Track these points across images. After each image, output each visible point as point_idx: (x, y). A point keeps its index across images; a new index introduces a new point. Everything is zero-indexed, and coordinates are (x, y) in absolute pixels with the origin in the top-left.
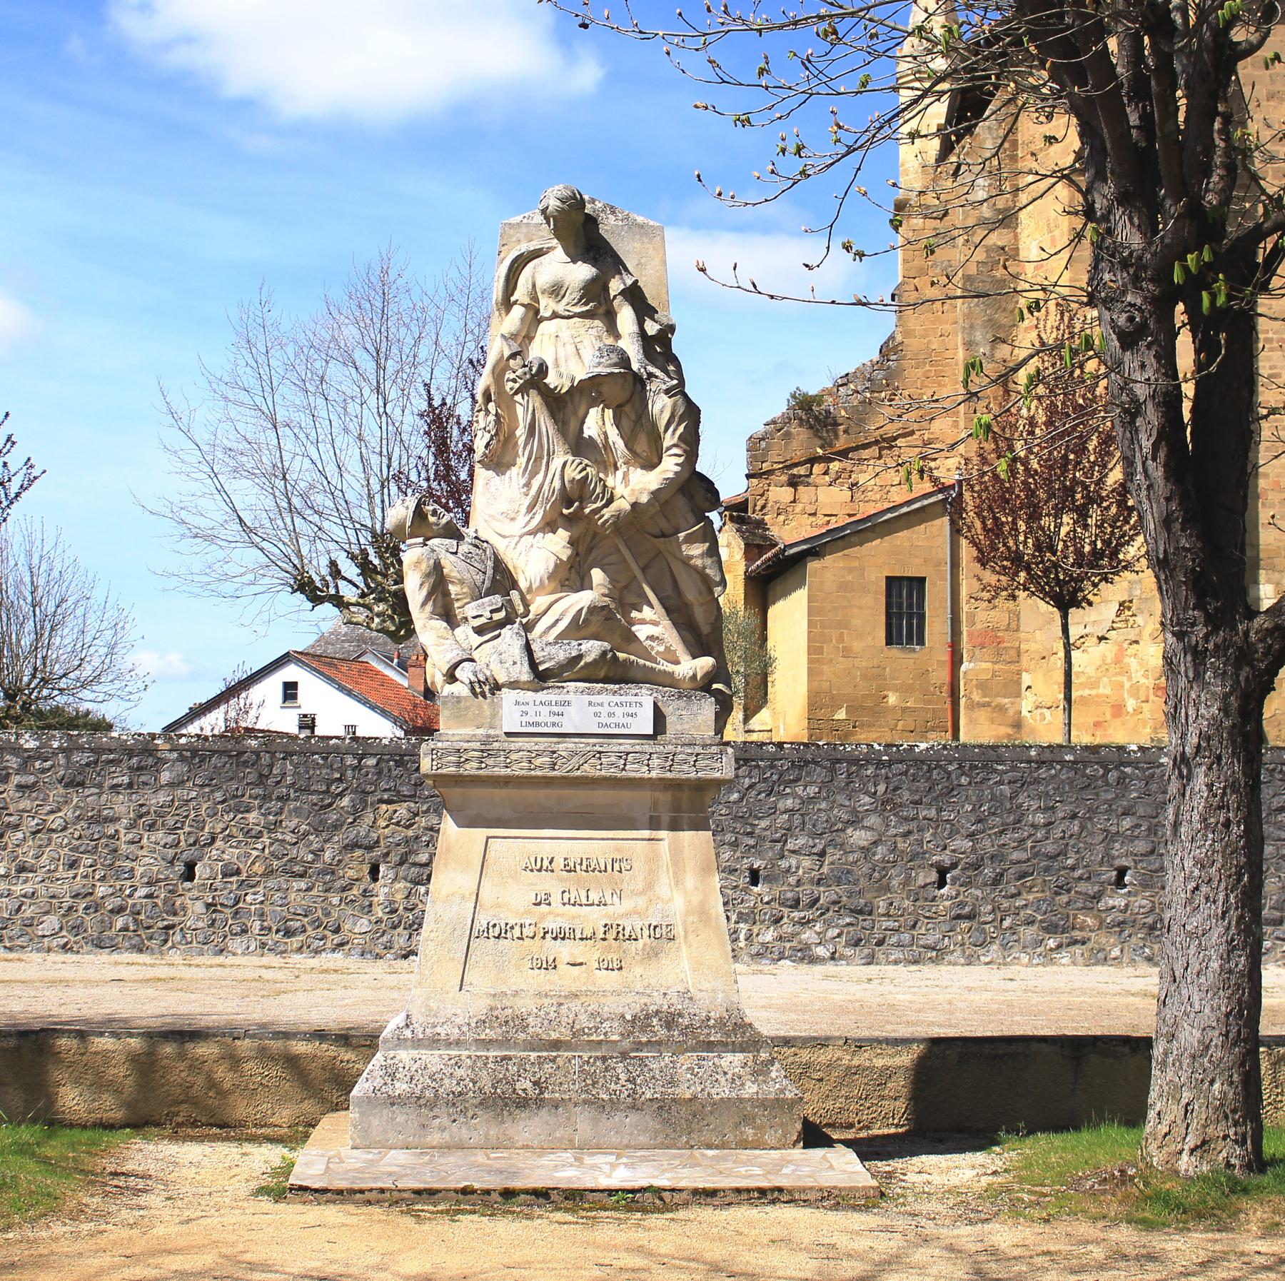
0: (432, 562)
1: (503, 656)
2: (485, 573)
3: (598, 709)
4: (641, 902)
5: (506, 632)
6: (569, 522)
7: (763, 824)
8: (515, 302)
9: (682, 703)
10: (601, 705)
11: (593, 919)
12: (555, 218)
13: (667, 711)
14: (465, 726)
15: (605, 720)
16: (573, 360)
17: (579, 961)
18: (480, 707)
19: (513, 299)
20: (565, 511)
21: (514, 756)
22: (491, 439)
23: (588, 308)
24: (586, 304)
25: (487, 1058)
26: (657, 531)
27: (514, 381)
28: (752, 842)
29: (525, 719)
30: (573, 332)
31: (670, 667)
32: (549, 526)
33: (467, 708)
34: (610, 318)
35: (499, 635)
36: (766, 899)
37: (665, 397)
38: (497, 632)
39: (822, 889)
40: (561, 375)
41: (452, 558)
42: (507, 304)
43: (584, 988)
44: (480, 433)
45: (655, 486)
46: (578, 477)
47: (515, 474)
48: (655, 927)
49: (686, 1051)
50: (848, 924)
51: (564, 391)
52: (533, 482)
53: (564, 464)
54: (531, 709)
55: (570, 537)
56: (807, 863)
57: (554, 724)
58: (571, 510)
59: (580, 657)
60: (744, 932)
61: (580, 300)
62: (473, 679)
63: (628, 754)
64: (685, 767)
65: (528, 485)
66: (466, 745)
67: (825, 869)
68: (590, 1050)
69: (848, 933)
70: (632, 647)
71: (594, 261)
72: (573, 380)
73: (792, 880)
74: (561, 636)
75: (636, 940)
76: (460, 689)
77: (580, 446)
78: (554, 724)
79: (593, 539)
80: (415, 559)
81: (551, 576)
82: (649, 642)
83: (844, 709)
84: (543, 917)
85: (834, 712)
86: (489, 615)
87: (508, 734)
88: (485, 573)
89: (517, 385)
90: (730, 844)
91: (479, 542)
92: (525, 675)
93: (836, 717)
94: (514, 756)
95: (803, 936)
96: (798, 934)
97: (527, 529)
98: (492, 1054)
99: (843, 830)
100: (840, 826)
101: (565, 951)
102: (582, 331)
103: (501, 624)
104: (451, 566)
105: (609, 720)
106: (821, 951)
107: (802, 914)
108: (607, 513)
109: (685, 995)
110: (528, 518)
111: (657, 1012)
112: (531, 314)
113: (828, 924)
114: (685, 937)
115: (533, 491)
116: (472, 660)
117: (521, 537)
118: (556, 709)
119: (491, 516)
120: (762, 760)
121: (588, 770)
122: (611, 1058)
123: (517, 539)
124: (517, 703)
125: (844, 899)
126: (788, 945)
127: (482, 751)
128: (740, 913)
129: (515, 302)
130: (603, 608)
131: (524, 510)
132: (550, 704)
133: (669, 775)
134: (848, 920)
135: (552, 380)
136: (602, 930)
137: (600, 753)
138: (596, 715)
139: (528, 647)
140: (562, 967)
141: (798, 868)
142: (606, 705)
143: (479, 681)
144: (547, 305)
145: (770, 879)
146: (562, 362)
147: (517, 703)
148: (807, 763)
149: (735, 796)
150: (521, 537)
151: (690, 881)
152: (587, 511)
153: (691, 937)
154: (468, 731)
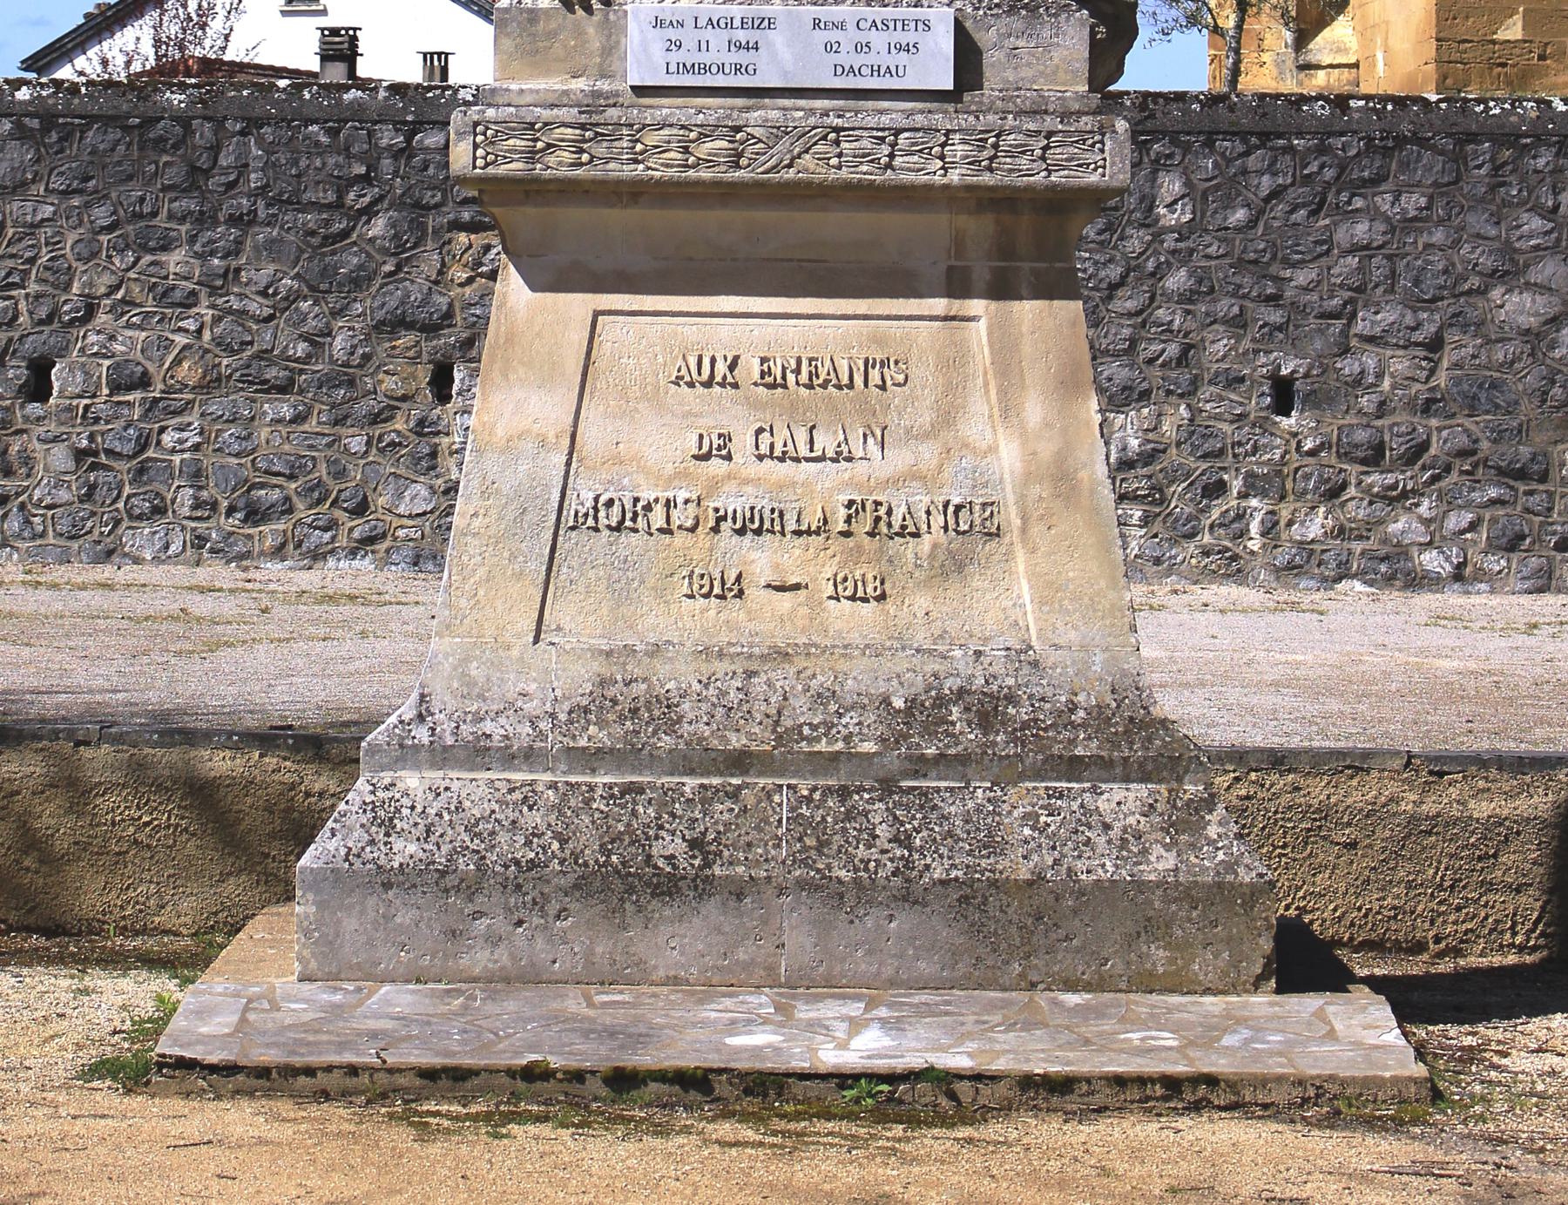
3: (834, 35)
4: (928, 454)
7: (1302, 277)
9: (1016, 23)
10: (841, 26)
11: (823, 489)
13: (986, 38)
14: (547, 73)
15: (847, 58)
17: (793, 580)
18: (579, 33)
21: (651, 139)
25: (591, 788)
28: (1276, 317)
29: (675, 57)
33: (552, 35)
36: (1309, 445)
39: (1434, 422)
43: (803, 640)
48: (958, 508)
49: (1023, 777)
50: (1494, 502)
54: (689, 36)
56: (1400, 364)
57: (738, 69)
60: (1258, 517)
63: (898, 132)
64: (1024, 162)
66: (547, 114)
67: (1441, 379)
68: (814, 774)
69: (1494, 520)
73: (1366, 402)
75: (916, 535)
78: (738, 69)
83: (1518, 20)
84: (714, 485)
85: (1496, 24)
87: (639, 91)
90: (1226, 321)
93: (1501, 35)
94: (651, 139)
95: (1394, 528)
96: (1381, 522)
98: (602, 779)
99: (1482, 292)
100: (1475, 282)
101: (761, 559)
105: (858, 60)
106: (1431, 561)
107: (1390, 479)
109: (1022, 655)
111: (961, 693)
113: (1449, 502)
118: (741, 36)
120: (1300, 135)
121: (810, 167)
122: (860, 790)
125: (1485, 445)
126: (1357, 547)
127: (583, 127)
128: (1250, 475)
132: (730, 24)
133: (987, 179)
134: (1493, 493)
136: (842, 513)
137: (837, 130)
138: (829, 48)
141: (1380, 376)
142: (851, 27)
145: (1315, 401)
148: (1401, 141)
149: (1240, 215)
151: (1034, 410)
153: (1036, 530)
154: (553, 84)
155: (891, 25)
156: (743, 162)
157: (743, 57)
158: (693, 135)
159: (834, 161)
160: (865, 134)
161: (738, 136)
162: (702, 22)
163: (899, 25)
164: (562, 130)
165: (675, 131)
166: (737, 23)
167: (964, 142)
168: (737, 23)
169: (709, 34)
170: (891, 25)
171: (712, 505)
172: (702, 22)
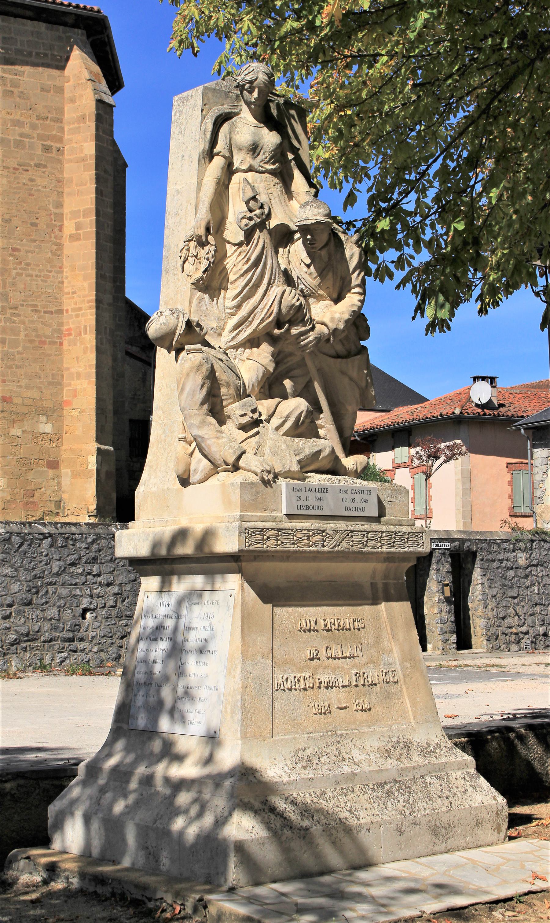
6: (273, 340)
8: (218, 154)
12: (259, 88)
15: (349, 504)
17: (343, 705)
19: (215, 151)
23: (274, 167)
24: (273, 164)
26: (332, 352)
29: (300, 503)
42: (210, 154)
48: (386, 673)
54: (303, 494)
57: (318, 508)
58: (283, 330)
59: (319, 452)
65: (238, 307)
66: (268, 525)
75: (375, 685)
78: (318, 508)
84: (315, 671)
105: (351, 505)
108: (312, 336)
114: (405, 680)
118: (319, 495)
124: (294, 490)
127: (278, 530)
129: (218, 154)
133: (393, 550)
136: (354, 678)
137: (352, 532)
140: (335, 712)
142: (349, 492)
144: (240, 160)
147: (294, 490)
151: (401, 635)
153: (408, 679)
156: (325, 544)
158: (311, 533)
159: (351, 544)
161: (324, 534)
162: (307, 490)
164: (273, 531)
165: (305, 532)
166: (317, 490)
167: (386, 536)
168: (317, 490)
169: (309, 494)
171: (318, 677)
172: (307, 490)
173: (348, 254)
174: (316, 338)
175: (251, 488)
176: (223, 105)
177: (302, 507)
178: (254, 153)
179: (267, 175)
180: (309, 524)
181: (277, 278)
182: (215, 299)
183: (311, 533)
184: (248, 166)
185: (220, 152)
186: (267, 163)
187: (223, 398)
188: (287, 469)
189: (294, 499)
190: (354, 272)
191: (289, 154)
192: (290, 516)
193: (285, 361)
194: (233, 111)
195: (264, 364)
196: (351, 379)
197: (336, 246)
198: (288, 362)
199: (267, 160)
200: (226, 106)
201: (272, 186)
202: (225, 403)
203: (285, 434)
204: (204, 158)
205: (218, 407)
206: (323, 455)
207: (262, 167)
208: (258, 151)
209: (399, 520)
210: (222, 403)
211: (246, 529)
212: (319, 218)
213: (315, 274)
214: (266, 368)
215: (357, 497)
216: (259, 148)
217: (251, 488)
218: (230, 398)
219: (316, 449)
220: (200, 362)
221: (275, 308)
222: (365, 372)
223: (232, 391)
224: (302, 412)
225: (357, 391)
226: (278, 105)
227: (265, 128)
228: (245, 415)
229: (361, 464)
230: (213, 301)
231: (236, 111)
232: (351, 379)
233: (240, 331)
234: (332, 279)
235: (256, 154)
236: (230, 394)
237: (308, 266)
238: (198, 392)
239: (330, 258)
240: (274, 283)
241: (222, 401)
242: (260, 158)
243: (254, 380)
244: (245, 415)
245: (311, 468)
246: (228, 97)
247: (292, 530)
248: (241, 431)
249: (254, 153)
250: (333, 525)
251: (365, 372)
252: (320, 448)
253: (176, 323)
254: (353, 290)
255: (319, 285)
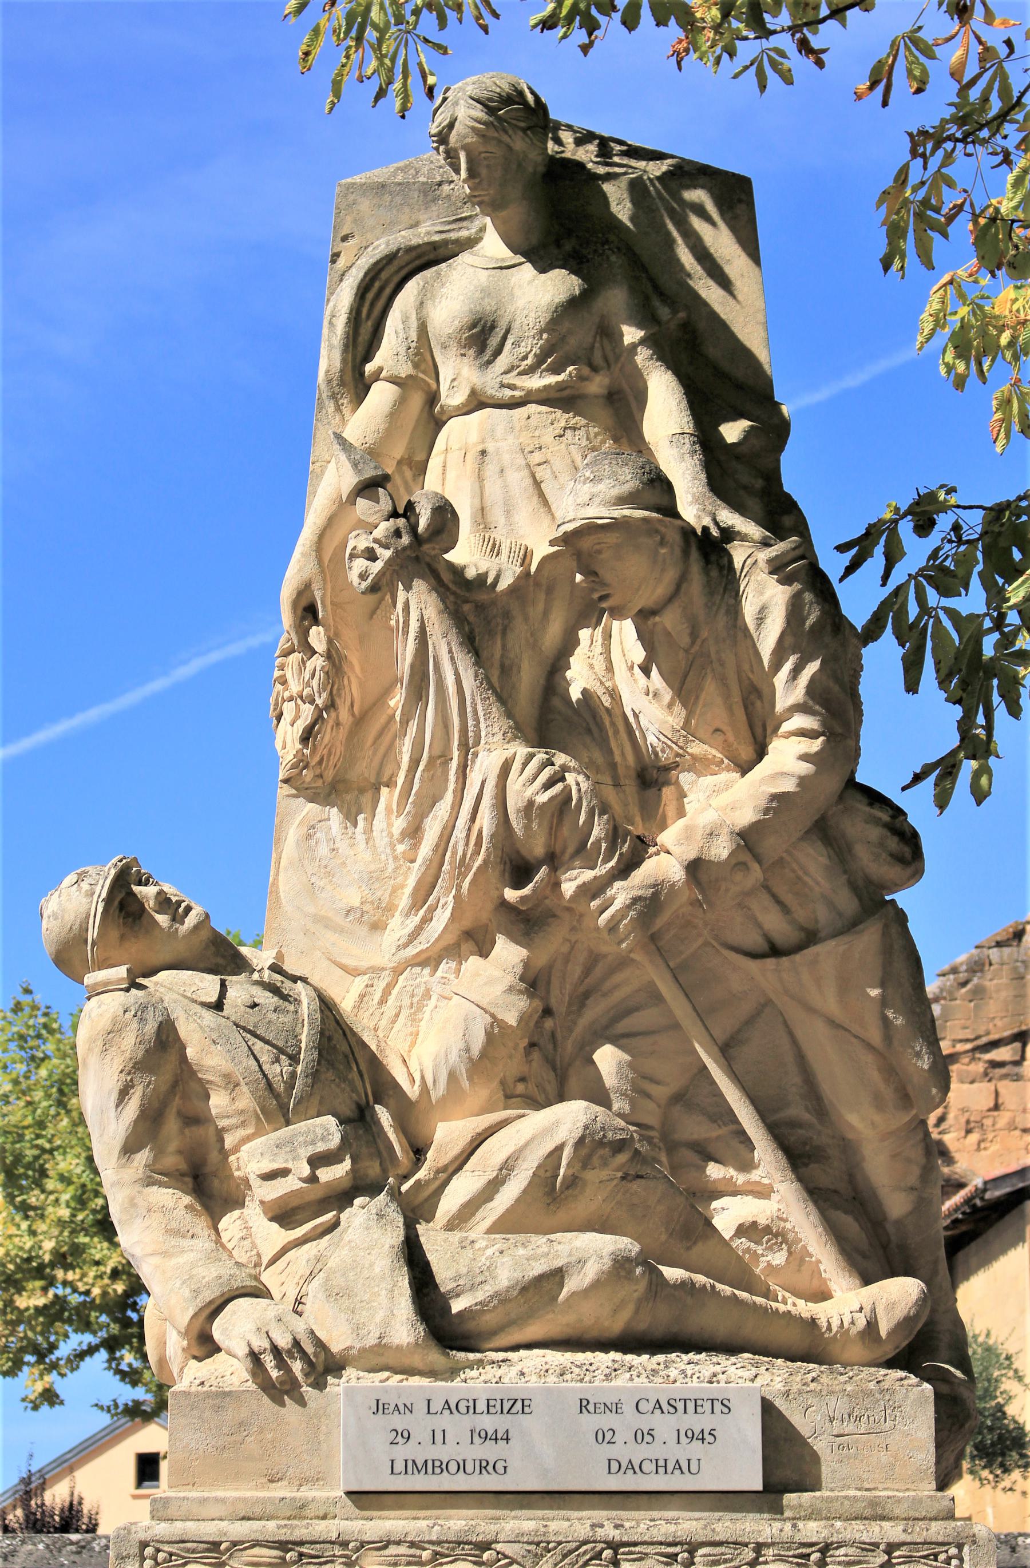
0: (151, 1027)
1: (348, 1281)
2: (294, 1059)
3: (605, 1421)
5: (359, 1214)
6: (525, 922)
12: (465, 147)
14: (236, 1477)
15: (624, 1451)
16: (525, 508)
19: (369, 368)
20: (511, 895)
22: (318, 719)
26: (754, 940)
27: (371, 556)
29: (403, 1452)
30: (525, 438)
31: (804, 1308)
32: (475, 940)
34: (622, 412)
35: (336, 1224)
37: (772, 581)
38: (329, 1216)
40: (495, 549)
41: (209, 1017)
44: (288, 708)
45: (746, 816)
46: (543, 798)
47: (388, 816)
51: (503, 585)
52: (428, 822)
53: (506, 771)
54: (419, 1424)
55: (527, 964)
57: (483, 1467)
58: (527, 890)
59: (557, 1276)
61: (540, 360)
62: (260, 1343)
63: (692, 1548)
65: (414, 833)
70: (701, 1251)
71: (575, 263)
72: (526, 556)
74: (504, 1226)
76: (229, 1370)
77: (555, 720)
78: (483, 1467)
79: (587, 971)
80: (105, 1023)
81: (479, 1064)
82: (742, 1244)
86: (306, 1171)
88: (294, 1059)
89: (377, 566)
91: (280, 983)
92: (403, 1326)
97: (411, 951)
102: (547, 437)
103: (342, 1198)
104: (204, 1046)
105: (639, 1453)
110: (416, 920)
112: (417, 401)
115: (426, 849)
116: (259, 1292)
117: (398, 971)
118: (488, 1423)
119: (318, 919)
123: (386, 978)
124: (380, 1407)
127: (283, 1546)
129: (376, 376)
130: (619, 1146)
131: (404, 901)
132: (472, 1408)
135: (466, 554)
137: (615, 1546)
138: (601, 1437)
139: (413, 1255)
142: (628, 1408)
143: (276, 1350)
146: (497, 516)
147: (380, 1407)
150: (398, 971)
152: (568, 888)
155: (680, 1406)
157: (490, 1451)
160: (649, 1549)
161: (486, 1556)
162: (437, 1406)
163: (691, 1406)
164: (257, 1551)
165: (403, 1550)
166: (481, 1406)
168: (481, 1406)
169: (446, 1421)
170: (680, 1406)
172: (437, 1406)
173: (749, 610)
174: (635, 900)
175: (217, 1409)
176: (416, 225)
177: (425, 1467)
178: (481, 351)
179: (532, 408)
180: (423, 1524)
181: (482, 726)
182: (361, 818)
183: (426, 1555)
184: (467, 392)
185: (380, 370)
186: (530, 371)
187: (221, 1123)
188: (371, 1341)
189: (379, 1441)
190: (777, 665)
191: (625, 329)
192: (362, 1498)
193: (607, 985)
194: (453, 236)
195: (484, 1004)
196: (833, 1024)
197: (710, 590)
198: (617, 987)
199: (529, 361)
200: (422, 230)
201: (548, 438)
202: (229, 1141)
203: (504, 1226)
204: (333, 397)
205: (214, 1156)
206: (572, 1285)
207: (512, 387)
208: (494, 341)
209: (874, 1503)
210: (221, 1141)
211: (144, 1545)
212: (591, 512)
213: (667, 695)
214: (493, 1016)
215: (665, 1425)
216: (499, 332)
217: (217, 1409)
218: (243, 1124)
219: (538, 1268)
220: (115, 1021)
221: (486, 821)
222: (874, 992)
223: (246, 1100)
224: (559, 1149)
225: (868, 1059)
226: (637, 188)
227: (529, 265)
228: (284, 1173)
229: (891, 1306)
230: (355, 825)
231: (464, 234)
232: (833, 1024)
233: (433, 909)
234: (719, 700)
235: (489, 352)
236: (241, 1112)
237: (646, 670)
238: (112, 1113)
239: (694, 635)
240: (477, 743)
241: (220, 1134)
242: (503, 361)
243: (454, 1057)
244: (284, 1173)
245: (534, 1331)
246: (434, 200)
247: (344, 1544)
248: (275, 1226)
249: (481, 351)
250: (529, 1526)
251: (874, 992)
252: (558, 1263)
253: (83, 909)
254: (787, 727)
255: (686, 726)
